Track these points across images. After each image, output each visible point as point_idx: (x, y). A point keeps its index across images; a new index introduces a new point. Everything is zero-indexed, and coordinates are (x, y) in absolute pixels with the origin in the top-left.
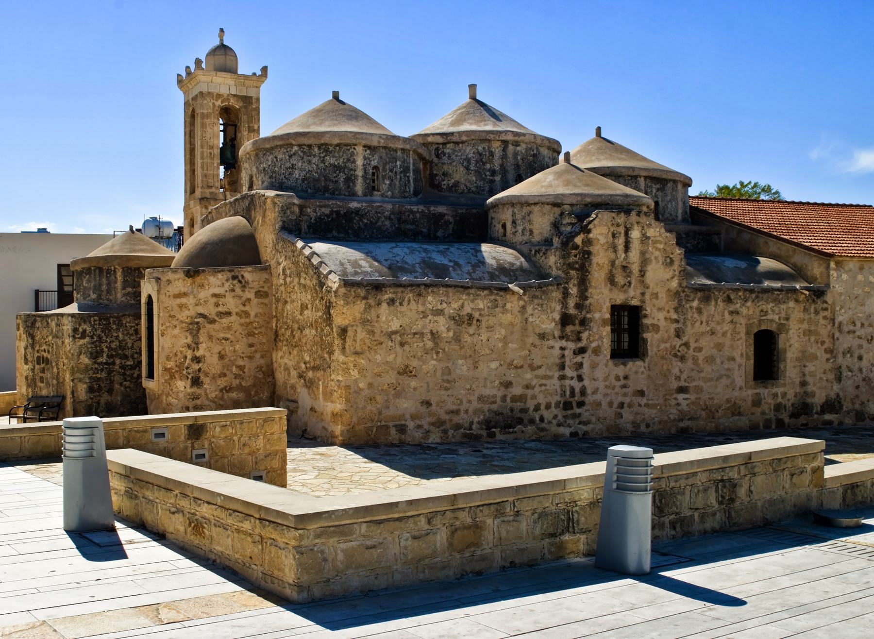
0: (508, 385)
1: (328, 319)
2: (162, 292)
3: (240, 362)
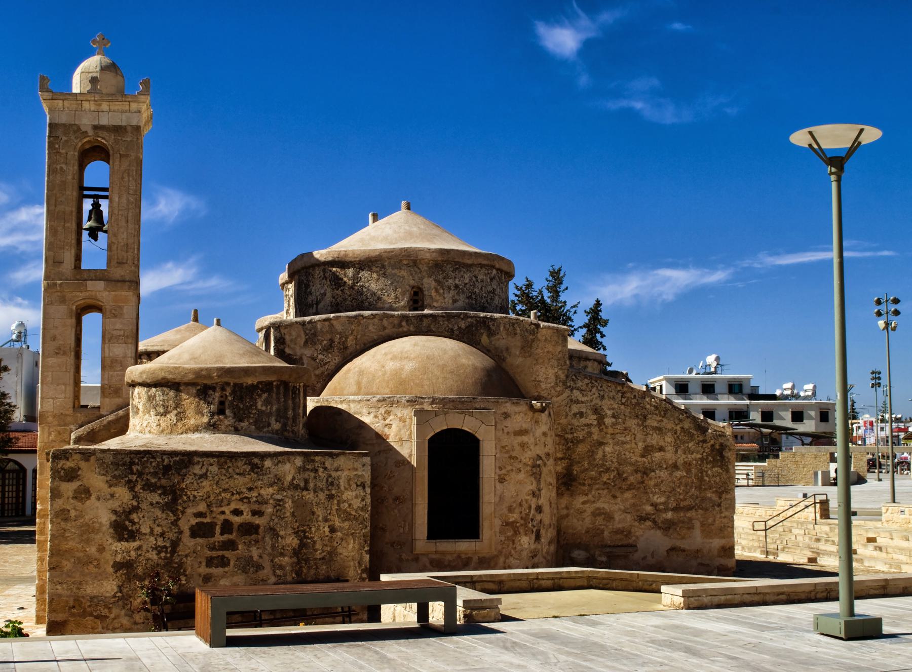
2: (499, 426)
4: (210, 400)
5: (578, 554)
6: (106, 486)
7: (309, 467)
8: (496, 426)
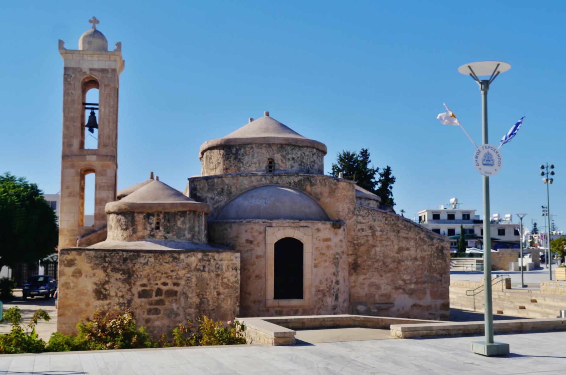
2: (314, 236)
4: (151, 221)
5: (361, 308)
6: (91, 269)
7: (206, 258)
8: (312, 236)
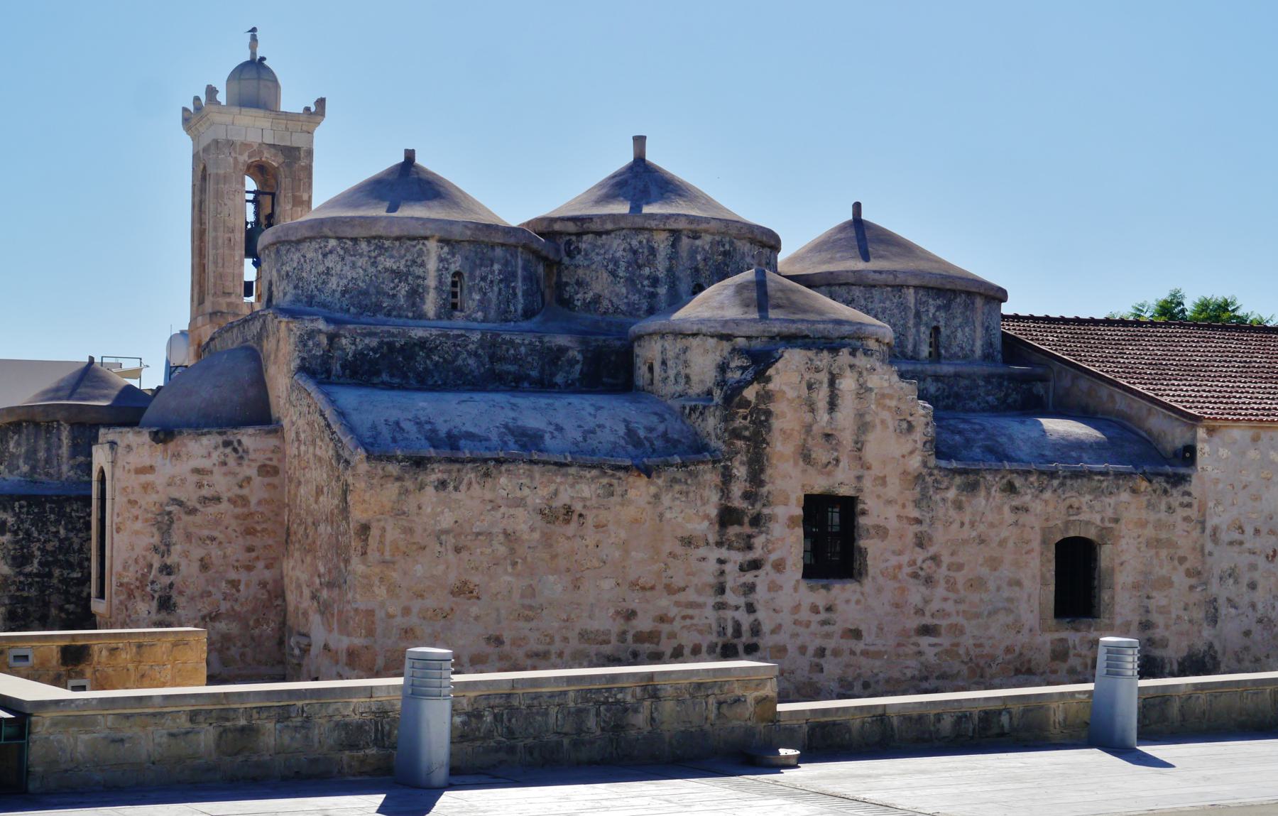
0: (630, 615)
1: (345, 510)
2: (120, 463)
3: (233, 575)
